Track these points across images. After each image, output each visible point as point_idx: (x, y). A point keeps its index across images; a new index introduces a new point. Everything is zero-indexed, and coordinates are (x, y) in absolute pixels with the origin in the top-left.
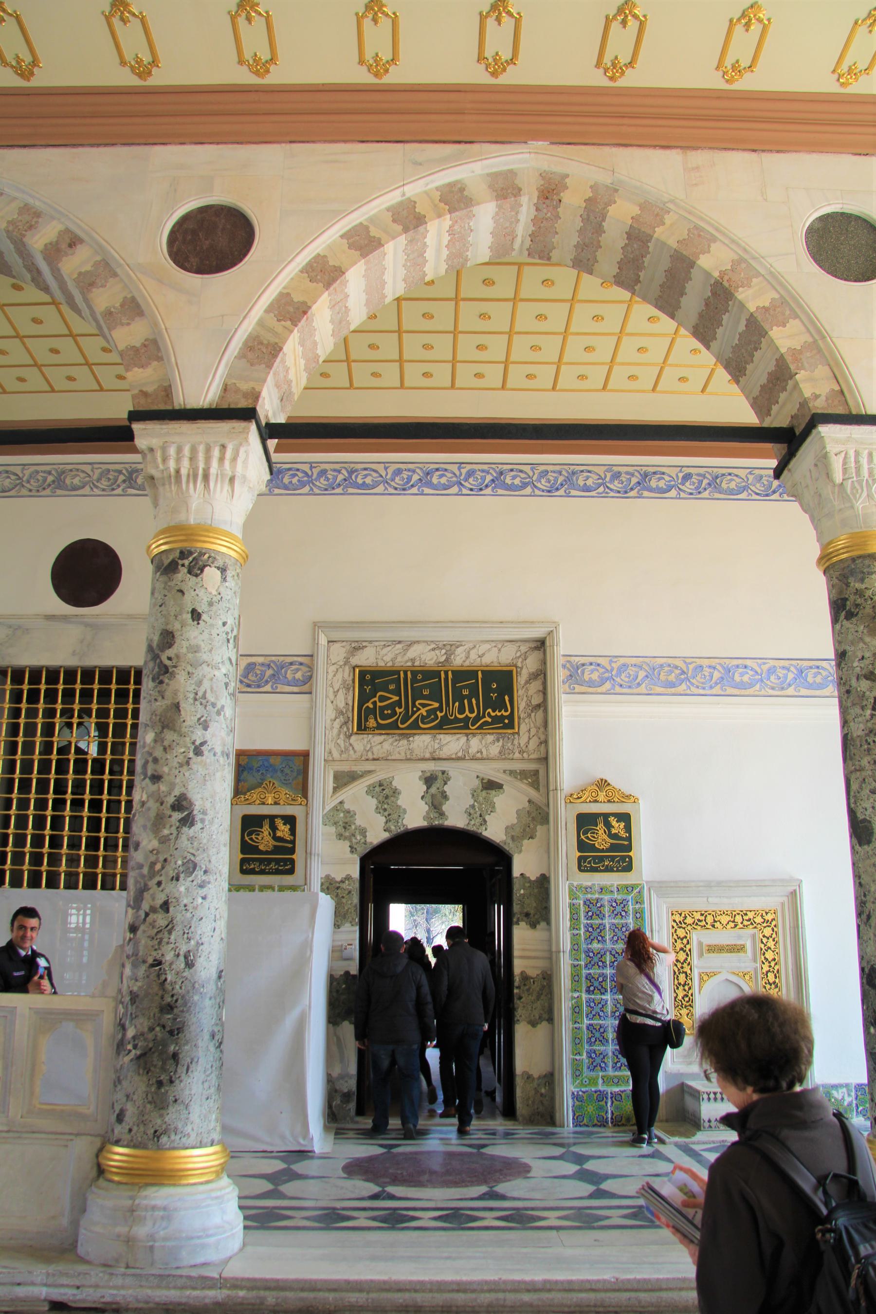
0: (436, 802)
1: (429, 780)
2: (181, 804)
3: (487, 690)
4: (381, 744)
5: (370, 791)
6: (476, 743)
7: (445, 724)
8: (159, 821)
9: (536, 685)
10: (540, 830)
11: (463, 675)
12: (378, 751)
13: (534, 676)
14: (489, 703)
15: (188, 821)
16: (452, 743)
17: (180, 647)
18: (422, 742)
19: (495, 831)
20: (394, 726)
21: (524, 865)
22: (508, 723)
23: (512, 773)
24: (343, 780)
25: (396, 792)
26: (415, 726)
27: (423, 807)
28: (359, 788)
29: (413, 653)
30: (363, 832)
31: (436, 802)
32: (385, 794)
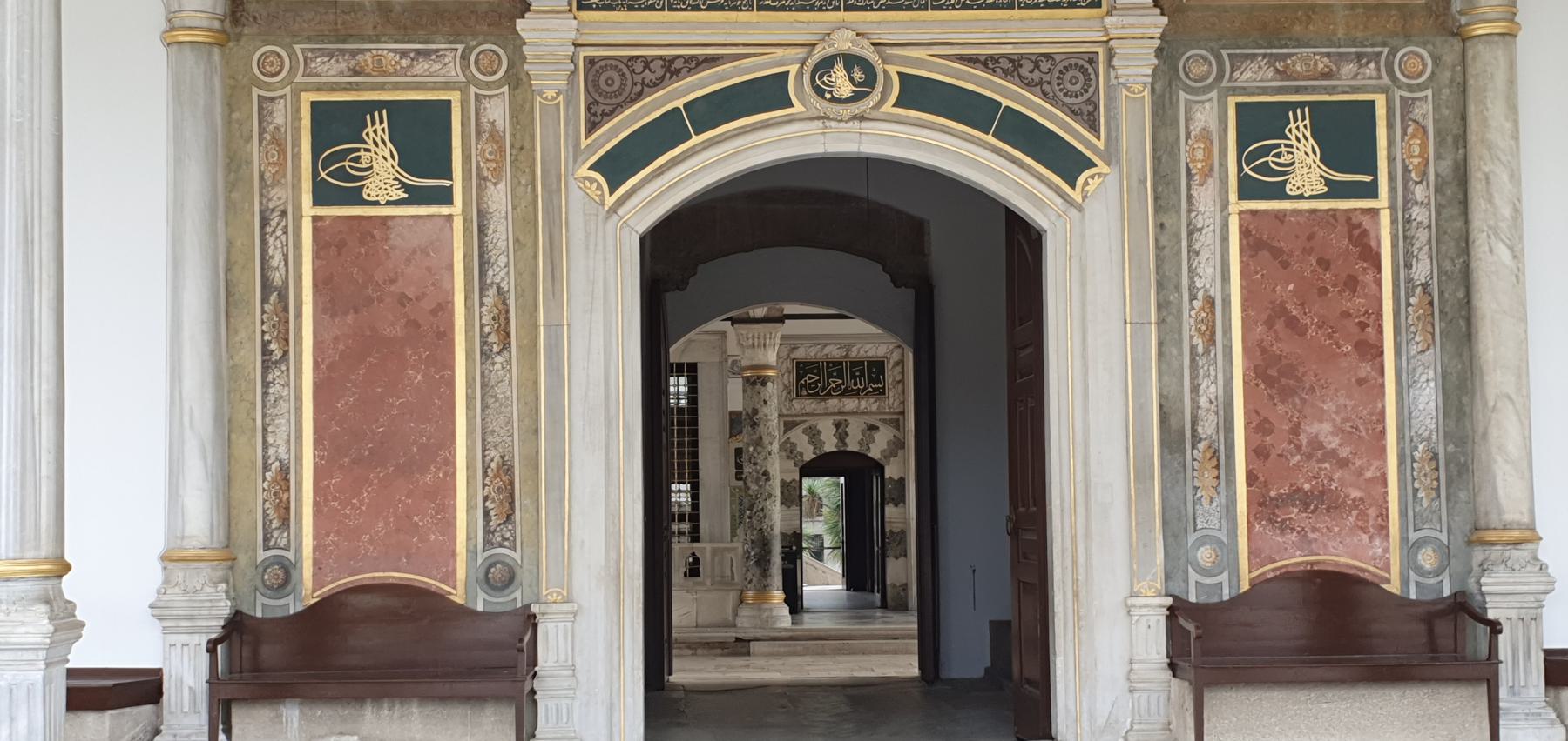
0: (842, 437)
1: (838, 425)
2: (766, 473)
3: (870, 372)
4: (810, 405)
5: (804, 432)
6: (863, 403)
7: (846, 393)
8: (758, 480)
9: (899, 369)
10: (900, 452)
11: (854, 364)
12: (809, 409)
13: (897, 364)
14: (871, 380)
15: (768, 479)
16: (850, 404)
17: (760, 415)
18: (833, 403)
19: (875, 453)
20: (817, 394)
21: (891, 472)
22: (881, 392)
23: (884, 421)
24: (789, 426)
25: (819, 432)
26: (829, 394)
27: (835, 440)
28: (798, 431)
29: (827, 350)
30: (801, 455)
31: (842, 437)
32: (813, 434)
